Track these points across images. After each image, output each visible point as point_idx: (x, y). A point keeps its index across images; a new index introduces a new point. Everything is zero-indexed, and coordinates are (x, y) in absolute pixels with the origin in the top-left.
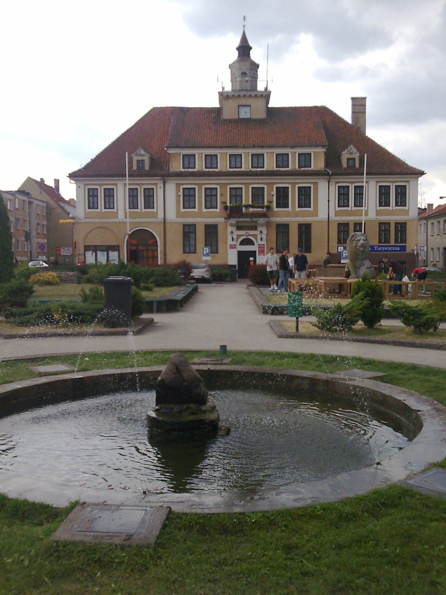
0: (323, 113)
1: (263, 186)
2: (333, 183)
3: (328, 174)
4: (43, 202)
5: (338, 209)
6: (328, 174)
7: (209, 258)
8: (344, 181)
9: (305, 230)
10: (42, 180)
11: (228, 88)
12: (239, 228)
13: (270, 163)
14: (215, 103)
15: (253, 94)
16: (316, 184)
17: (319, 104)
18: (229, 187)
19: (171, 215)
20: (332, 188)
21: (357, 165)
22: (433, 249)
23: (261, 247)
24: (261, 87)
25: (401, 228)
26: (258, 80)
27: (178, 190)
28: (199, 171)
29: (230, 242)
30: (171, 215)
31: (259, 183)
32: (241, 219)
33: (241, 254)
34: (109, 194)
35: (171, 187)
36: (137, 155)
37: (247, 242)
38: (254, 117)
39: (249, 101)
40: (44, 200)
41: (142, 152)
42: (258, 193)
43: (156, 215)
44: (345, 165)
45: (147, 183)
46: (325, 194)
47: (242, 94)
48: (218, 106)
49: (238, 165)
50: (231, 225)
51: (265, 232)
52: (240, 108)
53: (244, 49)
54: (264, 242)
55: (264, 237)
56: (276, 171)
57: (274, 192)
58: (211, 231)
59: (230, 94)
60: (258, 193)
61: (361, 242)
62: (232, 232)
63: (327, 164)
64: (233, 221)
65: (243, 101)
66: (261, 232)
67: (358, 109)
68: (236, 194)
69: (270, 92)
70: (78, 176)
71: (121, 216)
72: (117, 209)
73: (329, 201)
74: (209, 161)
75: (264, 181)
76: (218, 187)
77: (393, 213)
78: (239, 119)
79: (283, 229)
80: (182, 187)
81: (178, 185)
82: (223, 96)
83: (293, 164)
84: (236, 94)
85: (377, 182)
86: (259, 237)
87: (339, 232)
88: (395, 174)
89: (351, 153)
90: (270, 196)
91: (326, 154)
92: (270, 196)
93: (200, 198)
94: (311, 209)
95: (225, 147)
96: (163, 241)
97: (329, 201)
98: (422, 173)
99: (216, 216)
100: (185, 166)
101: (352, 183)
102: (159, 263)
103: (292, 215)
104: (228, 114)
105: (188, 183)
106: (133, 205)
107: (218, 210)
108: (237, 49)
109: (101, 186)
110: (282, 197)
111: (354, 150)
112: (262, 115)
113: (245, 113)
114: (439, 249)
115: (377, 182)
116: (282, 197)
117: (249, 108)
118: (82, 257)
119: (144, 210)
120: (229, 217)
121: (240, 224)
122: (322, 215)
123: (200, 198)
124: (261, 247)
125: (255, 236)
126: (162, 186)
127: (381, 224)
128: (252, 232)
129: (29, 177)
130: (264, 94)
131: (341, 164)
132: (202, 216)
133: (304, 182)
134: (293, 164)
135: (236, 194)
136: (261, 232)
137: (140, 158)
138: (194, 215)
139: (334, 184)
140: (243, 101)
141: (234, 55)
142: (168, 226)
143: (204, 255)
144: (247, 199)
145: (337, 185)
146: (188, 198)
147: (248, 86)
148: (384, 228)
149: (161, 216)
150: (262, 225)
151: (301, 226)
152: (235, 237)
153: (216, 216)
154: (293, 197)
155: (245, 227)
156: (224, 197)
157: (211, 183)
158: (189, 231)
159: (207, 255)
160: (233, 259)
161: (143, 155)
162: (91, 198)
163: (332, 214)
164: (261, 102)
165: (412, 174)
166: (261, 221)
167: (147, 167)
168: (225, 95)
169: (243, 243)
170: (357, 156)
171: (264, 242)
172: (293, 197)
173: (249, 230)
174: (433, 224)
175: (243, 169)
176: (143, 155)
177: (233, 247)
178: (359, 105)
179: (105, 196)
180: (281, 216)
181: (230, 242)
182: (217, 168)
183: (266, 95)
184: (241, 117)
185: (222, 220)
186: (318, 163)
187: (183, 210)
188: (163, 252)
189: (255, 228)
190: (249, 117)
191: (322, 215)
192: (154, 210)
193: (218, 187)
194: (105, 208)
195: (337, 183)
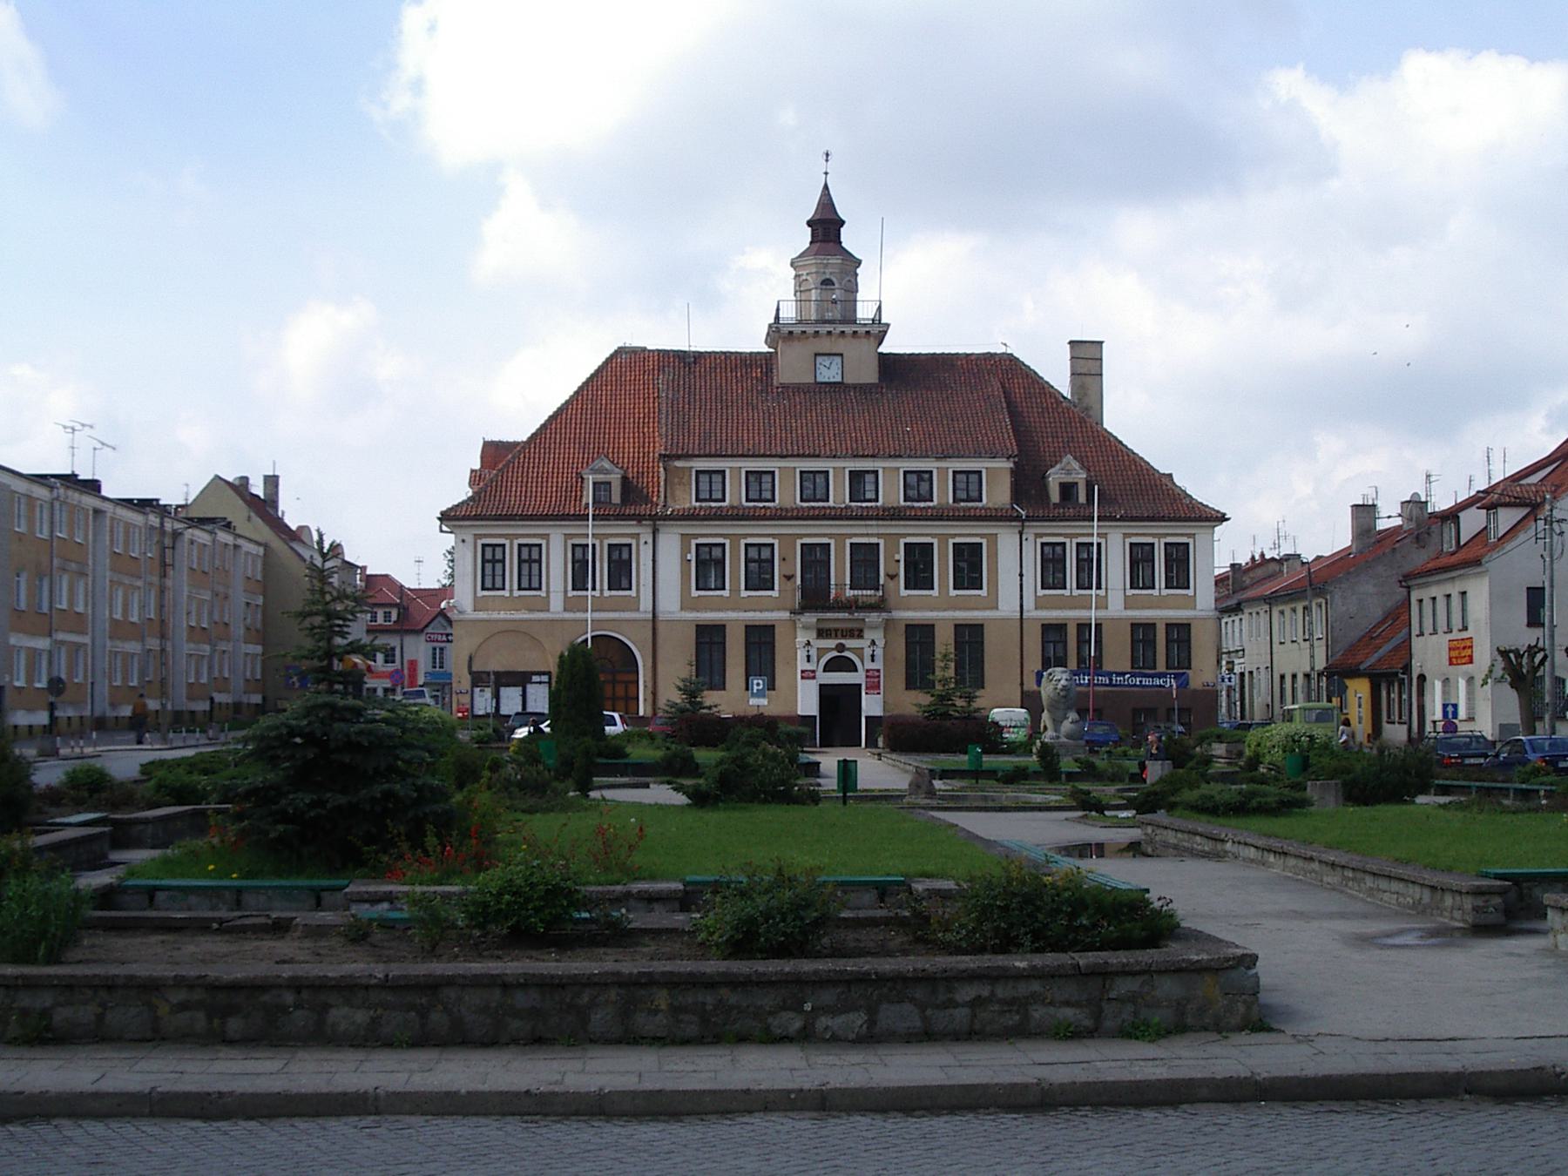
0: (1003, 372)
1: (874, 540)
2: (1029, 534)
3: (1018, 518)
4: (259, 544)
5: (1041, 592)
6: (1018, 518)
7: (764, 702)
8: (1056, 532)
9: (970, 637)
10: (245, 480)
11: (789, 313)
12: (822, 633)
13: (891, 492)
14: (754, 341)
15: (848, 329)
16: (993, 539)
17: (1000, 350)
18: (799, 542)
19: (670, 604)
20: (1029, 548)
21: (1082, 499)
22: (1282, 677)
23: (872, 675)
24: (864, 312)
25: (1180, 633)
26: (859, 296)
27: (685, 549)
28: (732, 507)
29: (802, 664)
30: (670, 604)
31: (867, 535)
32: (829, 615)
33: (828, 695)
34: (531, 559)
35: (670, 541)
36: (594, 471)
37: (840, 664)
38: (849, 380)
39: (840, 346)
40: (260, 540)
41: (607, 465)
42: (865, 557)
43: (634, 604)
44: (1055, 496)
45: (619, 532)
46: (1013, 560)
47: (824, 329)
48: (765, 349)
49: (820, 493)
50: (806, 628)
51: (881, 643)
52: (819, 359)
53: (826, 226)
54: (878, 665)
55: (879, 652)
56: (906, 508)
57: (901, 556)
58: (761, 640)
59: (797, 330)
60: (865, 557)
61: (1063, 682)
62: (808, 643)
63: (1018, 494)
64: (810, 618)
65: (825, 345)
66: (873, 643)
67: (1084, 367)
68: (815, 558)
69: (888, 325)
70: (464, 518)
71: (556, 603)
72: (548, 592)
73: (1021, 575)
74: (754, 486)
75: (875, 531)
76: (776, 542)
77: (1160, 603)
78: (817, 383)
79: (919, 636)
80: (694, 542)
81: (686, 538)
82: (778, 333)
83: (943, 494)
84: (810, 330)
85: (1126, 535)
86: (868, 652)
87: (1044, 643)
88: (1162, 519)
89: (1069, 473)
90: (892, 561)
91: (1014, 473)
92: (892, 561)
93: (735, 568)
94: (983, 592)
95: (792, 456)
96: (650, 664)
97: (1021, 575)
98: (1222, 518)
99: (771, 607)
100: (702, 496)
101: (1071, 536)
102: (641, 713)
103: (940, 606)
104: (792, 369)
105: (710, 533)
106: (579, 582)
107: (775, 594)
108: (809, 223)
109: (511, 537)
110: (919, 567)
111: (1076, 465)
112: (870, 375)
113: (829, 372)
114: (1294, 676)
115: (1126, 535)
116: (919, 567)
117: (838, 359)
118: (466, 699)
119: (607, 593)
120: (805, 608)
121: (822, 626)
122: (1008, 606)
123: (735, 568)
124: (872, 675)
125: (859, 652)
126: (650, 541)
127: (1135, 626)
128: (849, 643)
129: (217, 477)
130: (875, 330)
131: (1048, 497)
132: (736, 608)
133: (967, 533)
134: (943, 494)
135: (815, 558)
136: (873, 643)
137: (600, 478)
138: (722, 605)
139: (1031, 538)
140: (825, 345)
141: (804, 238)
142: (661, 628)
143: (753, 695)
144: (840, 571)
145: (1039, 541)
146: (708, 567)
147: (835, 313)
148: (1142, 633)
149: (646, 603)
150: (874, 627)
151: (959, 628)
152: (813, 653)
153: (771, 607)
154: (943, 566)
155: (836, 630)
156: (788, 565)
157: (760, 533)
158: (709, 638)
159: (760, 694)
160: (807, 703)
161: (607, 472)
162: (489, 566)
163: (1029, 603)
164: (865, 346)
165: (1200, 519)
166: (873, 617)
167: (616, 498)
168: (785, 330)
169: (831, 666)
170: (1080, 477)
171: (878, 665)
172: (943, 566)
173: (844, 637)
174: (1282, 613)
175: (831, 503)
176: (607, 472)
177: (808, 675)
178: (1086, 357)
179: (520, 561)
180: (913, 607)
181: (802, 664)
182: (773, 500)
183: (878, 330)
184: (820, 379)
185: (786, 615)
186: (997, 493)
187: (695, 593)
188: (650, 685)
189: (859, 634)
190: (838, 379)
191: (1008, 606)
192: (633, 593)
193: (776, 542)
194: (520, 589)
195: (1037, 535)
